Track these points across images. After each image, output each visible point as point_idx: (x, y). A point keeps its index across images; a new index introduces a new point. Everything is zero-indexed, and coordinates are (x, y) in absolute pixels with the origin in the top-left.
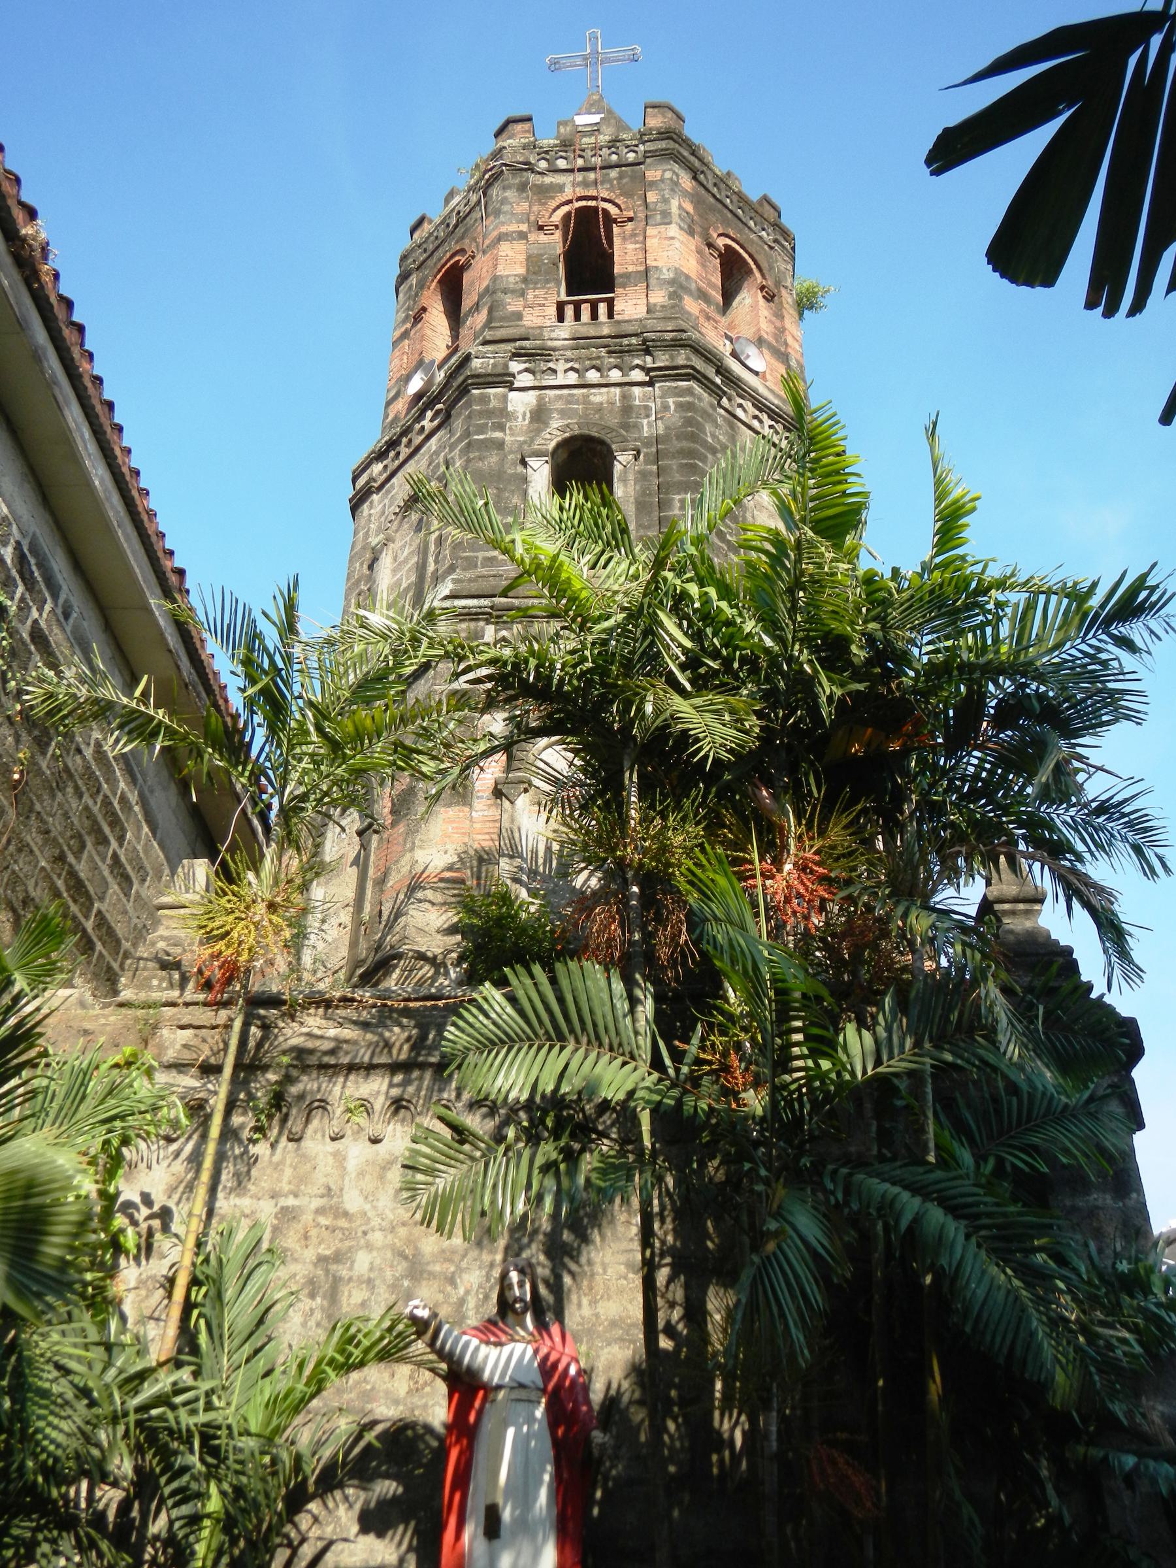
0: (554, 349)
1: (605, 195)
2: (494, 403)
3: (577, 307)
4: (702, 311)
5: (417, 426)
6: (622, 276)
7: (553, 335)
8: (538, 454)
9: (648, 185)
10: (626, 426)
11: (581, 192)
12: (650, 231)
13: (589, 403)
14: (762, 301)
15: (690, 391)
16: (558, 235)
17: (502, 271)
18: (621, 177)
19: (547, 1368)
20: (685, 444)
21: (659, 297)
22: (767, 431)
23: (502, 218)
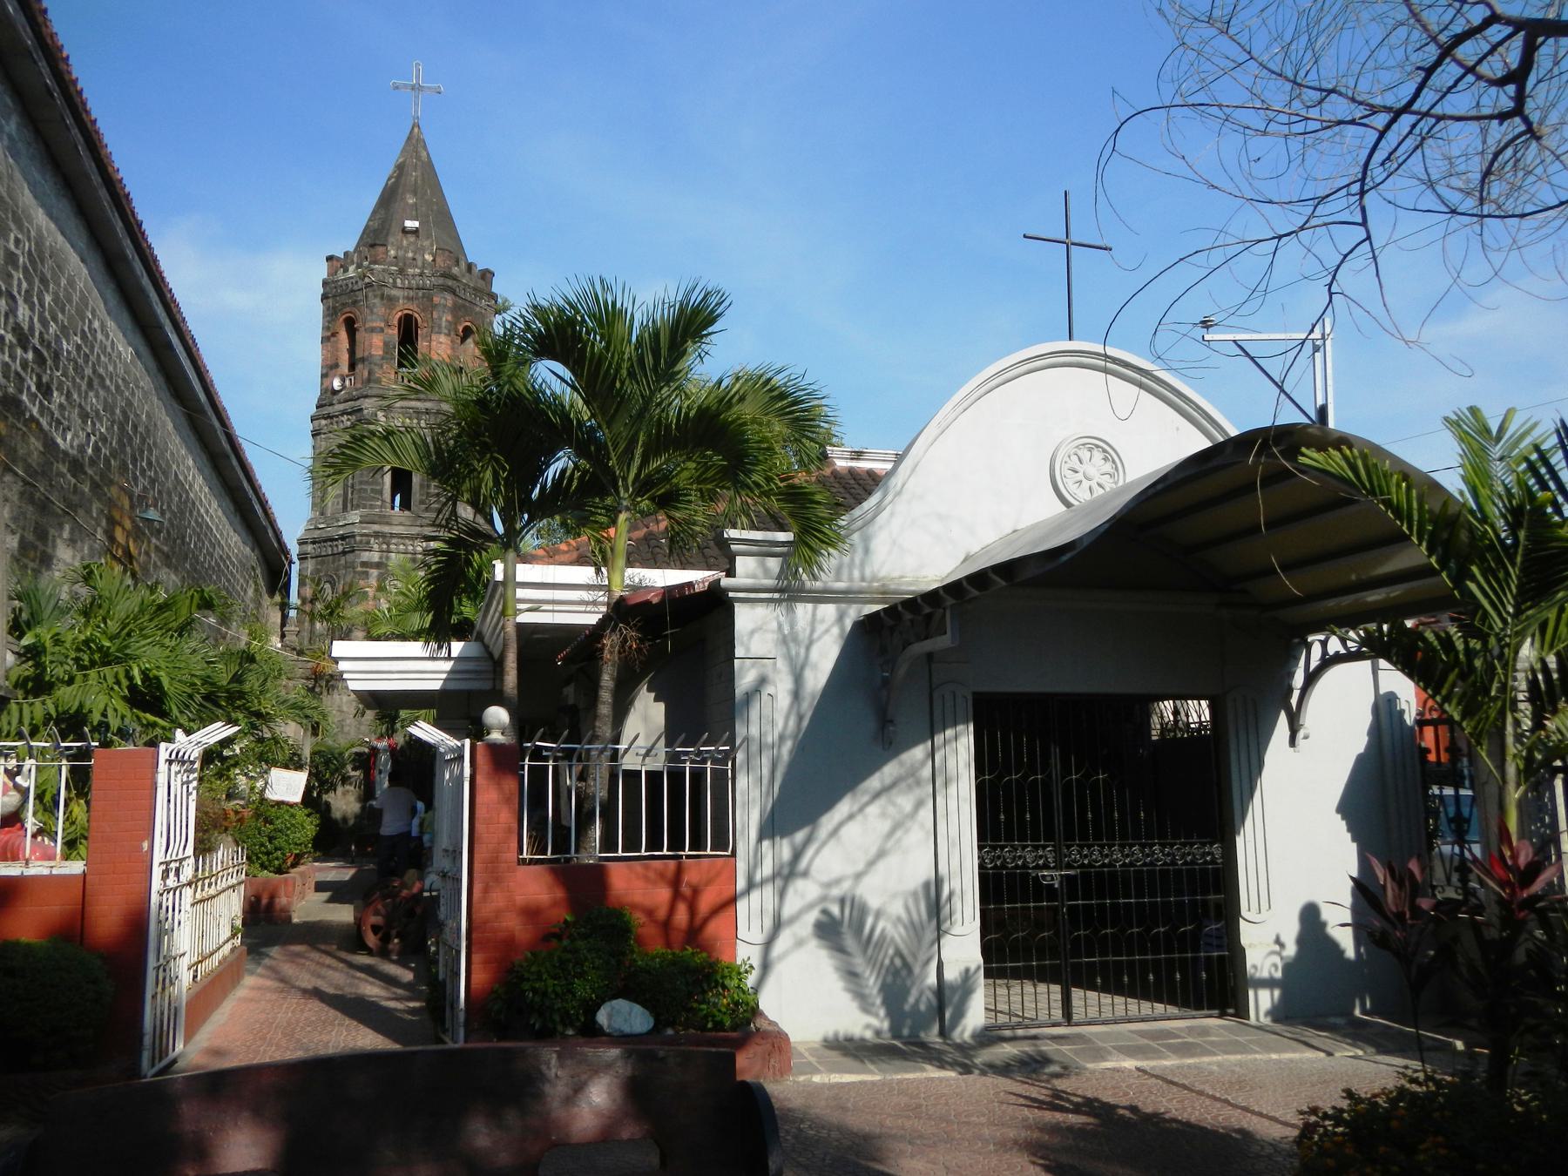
12: (434, 337)
19: (390, 746)
23: (374, 317)
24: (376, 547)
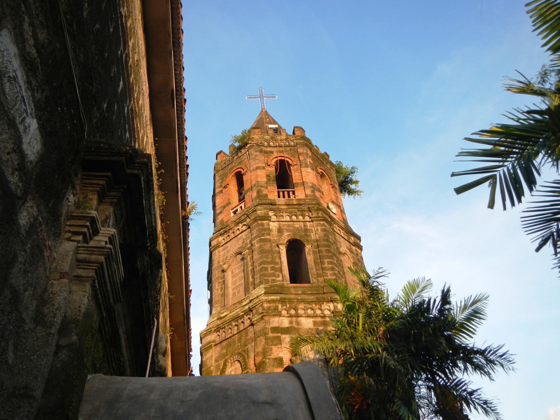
0: (282, 209)
1: (287, 156)
2: (266, 226)
3: (283, 192)
4: (320, 195)
5: (236, 228)
6: (296, 183)
7: (280, 203)
8: (281, 244)
9: (299, 154)
10: (306, 235)
11: (280, 155)
12: (303, 169)
13: (295, 227)
14: (331, 189)
15: (324, 225)
16: (274, 169)
17: (259, 180)
18: (291, 150)
20: (326, 243)
21: (309, 192)
22: (342, 235)
24: (284, 312)
